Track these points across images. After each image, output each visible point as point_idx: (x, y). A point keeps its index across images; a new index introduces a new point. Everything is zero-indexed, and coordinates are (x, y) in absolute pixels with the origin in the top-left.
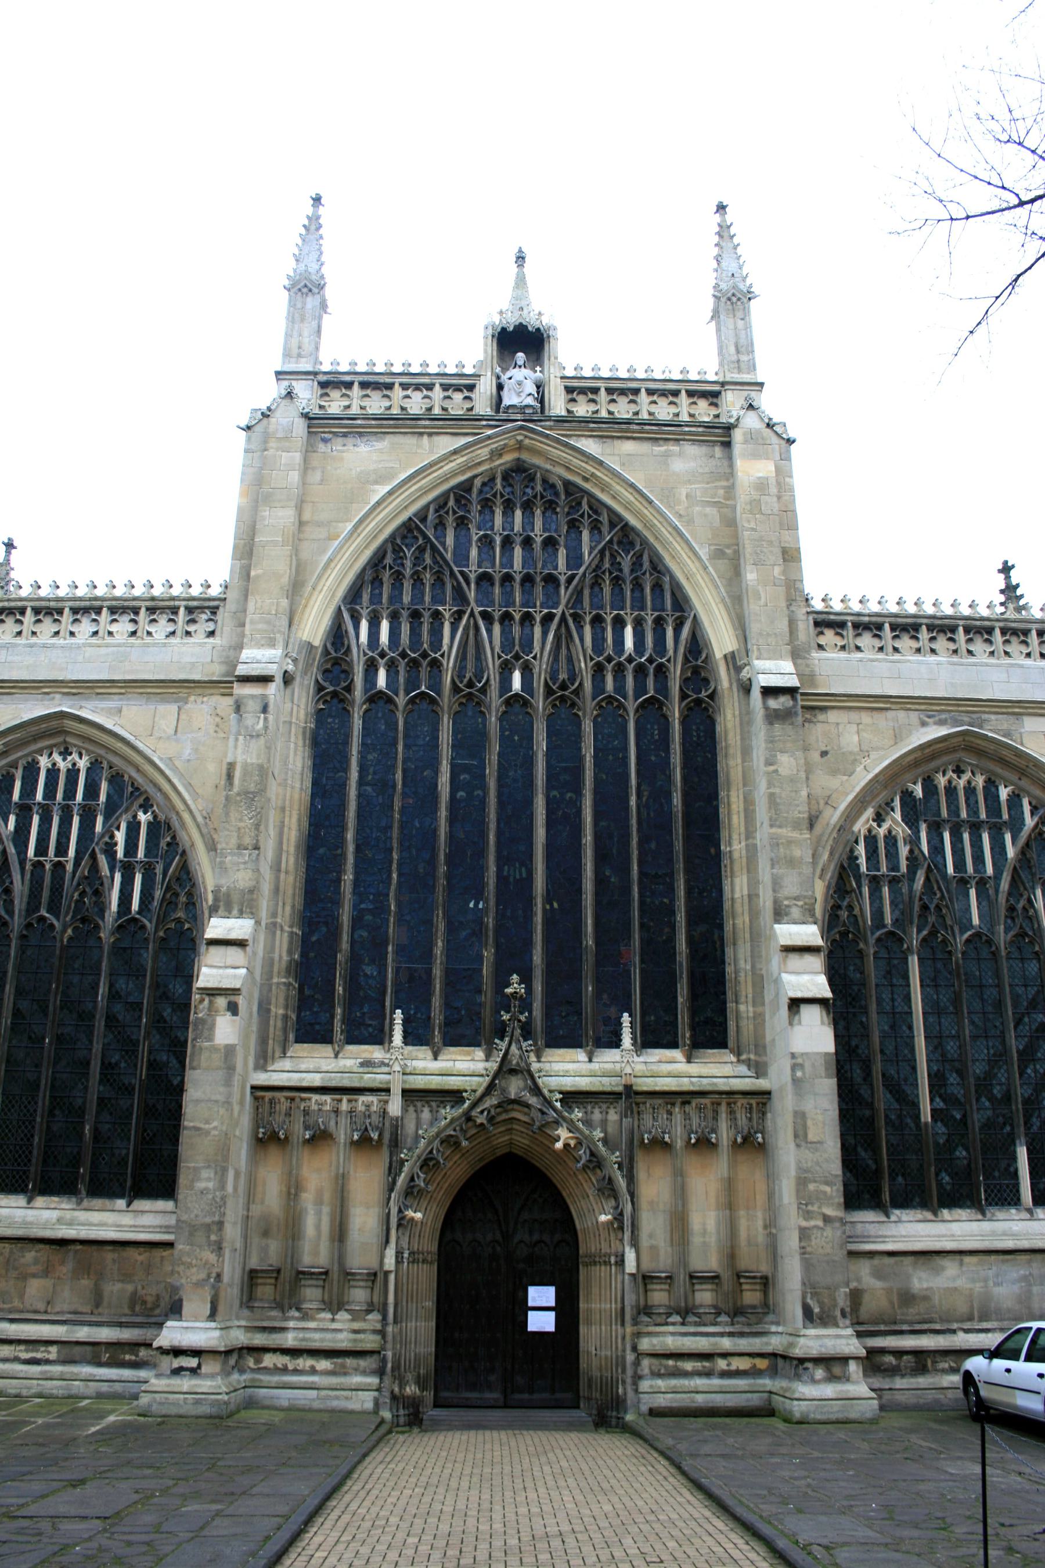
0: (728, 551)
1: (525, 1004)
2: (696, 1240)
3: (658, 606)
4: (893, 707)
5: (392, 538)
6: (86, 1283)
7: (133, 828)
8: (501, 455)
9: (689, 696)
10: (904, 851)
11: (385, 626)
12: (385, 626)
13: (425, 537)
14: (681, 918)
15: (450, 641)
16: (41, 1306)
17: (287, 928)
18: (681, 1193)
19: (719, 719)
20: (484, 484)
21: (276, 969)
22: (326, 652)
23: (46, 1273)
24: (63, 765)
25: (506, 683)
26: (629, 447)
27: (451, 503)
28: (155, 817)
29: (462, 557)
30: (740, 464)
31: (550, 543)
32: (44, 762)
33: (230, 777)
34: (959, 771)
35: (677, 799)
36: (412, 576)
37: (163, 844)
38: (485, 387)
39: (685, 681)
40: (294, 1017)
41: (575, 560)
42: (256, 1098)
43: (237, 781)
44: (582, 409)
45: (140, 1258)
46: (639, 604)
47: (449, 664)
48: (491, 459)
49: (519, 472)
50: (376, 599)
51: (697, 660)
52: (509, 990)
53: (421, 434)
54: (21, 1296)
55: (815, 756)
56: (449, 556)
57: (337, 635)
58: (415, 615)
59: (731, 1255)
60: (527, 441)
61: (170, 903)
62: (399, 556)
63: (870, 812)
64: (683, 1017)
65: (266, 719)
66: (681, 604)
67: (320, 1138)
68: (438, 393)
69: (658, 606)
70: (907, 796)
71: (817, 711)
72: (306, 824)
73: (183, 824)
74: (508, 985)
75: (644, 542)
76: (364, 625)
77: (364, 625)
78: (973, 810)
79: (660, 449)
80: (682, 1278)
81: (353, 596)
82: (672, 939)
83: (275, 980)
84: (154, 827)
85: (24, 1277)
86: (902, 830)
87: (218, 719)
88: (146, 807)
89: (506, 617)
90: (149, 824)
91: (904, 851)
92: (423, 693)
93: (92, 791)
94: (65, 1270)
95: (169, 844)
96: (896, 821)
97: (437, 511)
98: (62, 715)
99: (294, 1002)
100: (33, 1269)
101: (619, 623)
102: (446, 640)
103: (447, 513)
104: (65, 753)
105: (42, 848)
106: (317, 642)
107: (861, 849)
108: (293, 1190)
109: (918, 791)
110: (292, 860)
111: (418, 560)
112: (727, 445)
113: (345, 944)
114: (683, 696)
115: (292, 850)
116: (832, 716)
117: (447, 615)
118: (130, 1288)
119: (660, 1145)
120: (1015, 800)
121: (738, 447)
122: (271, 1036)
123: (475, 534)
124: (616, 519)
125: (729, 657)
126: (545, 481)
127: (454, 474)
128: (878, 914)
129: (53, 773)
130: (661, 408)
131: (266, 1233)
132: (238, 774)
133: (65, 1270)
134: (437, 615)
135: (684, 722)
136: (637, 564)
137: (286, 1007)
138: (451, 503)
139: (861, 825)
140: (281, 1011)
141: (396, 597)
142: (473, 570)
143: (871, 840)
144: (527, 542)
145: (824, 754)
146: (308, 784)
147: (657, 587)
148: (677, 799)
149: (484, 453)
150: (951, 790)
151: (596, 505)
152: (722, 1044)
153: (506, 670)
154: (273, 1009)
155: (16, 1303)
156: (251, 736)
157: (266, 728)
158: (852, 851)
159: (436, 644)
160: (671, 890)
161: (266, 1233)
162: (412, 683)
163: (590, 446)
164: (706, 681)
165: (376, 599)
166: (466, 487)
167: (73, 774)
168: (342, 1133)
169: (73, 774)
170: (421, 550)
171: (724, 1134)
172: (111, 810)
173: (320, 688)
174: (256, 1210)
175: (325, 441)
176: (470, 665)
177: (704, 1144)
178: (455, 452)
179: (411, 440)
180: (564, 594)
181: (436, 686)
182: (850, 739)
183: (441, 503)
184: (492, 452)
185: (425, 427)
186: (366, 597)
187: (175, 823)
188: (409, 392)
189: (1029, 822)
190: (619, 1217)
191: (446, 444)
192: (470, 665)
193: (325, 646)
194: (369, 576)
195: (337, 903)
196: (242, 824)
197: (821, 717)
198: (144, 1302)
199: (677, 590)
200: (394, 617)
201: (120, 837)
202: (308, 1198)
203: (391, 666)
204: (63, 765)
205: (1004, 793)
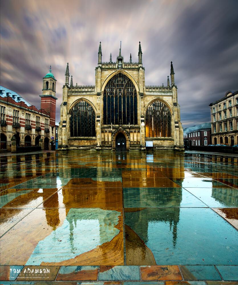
1: (121, 122)
2: (135, 139)
3: (132, 87)
5: (109, 81)
6: (90, 143)
7: (89, 107)
10: (152, 108)
11: (109, 89)
12: (109, 89)
14: (134, 114)
15: (114, 91)
18: (133, 136)
22: (104, 92)
23: (87, 142)
24: (83, 102)
25: (119, 94)
29: (115, 83)
30: (140, 73)
31: (123, 81)
32: (81, 102)
33: (97, 104)
34: (158, 101)
38: (117, 65)
39: (134, 94)
41: (125, 83)
42: (101, 129)
44: (126, 67)
46: (131, 87)
47: (114, 93)
49: (120, 74)
50: (108, 87)
55: (145, 100)
57: (105, 90)
58: (111, 88)
59: (137, 140)
61: (93, 114)
62: (110, 83)
63: (150, 105)
64: (134, 122)
66: (134, 86)
67: (106, 132)
69: (132, 87)
70: (153, 104)
76: (107, 89)
77: (107, 89)
78: (159, 105)
79: (133, 71)
80: (133, 142)
81: (106, 87)
82: (133, 116)
84: (91, 107)
85: (85, 143)
86: (152, 107)
88: (90, 106)
89: (119, 88)
91: (152, 108)
93: (85, 104)
96: (152, 106)
98: (82, 98)
101: (129, 88)
104: (83, 101)
105: (82, 110)
107: (149, 108)
108: (104, 136)
109: (154, 103)
111: (111, 83)
112: (139, 71)
113: (107, 117)
116: (147, 97)
119: (132, 132)
120: (162, 104)
121: (140, 72)
123: (116, 80)
124: (129, 78)
128: (150, 114)
129: (82, 103)
131: (103, 139)
133: (88, 142)
134: (113, 88)
135: (134, 97)
136: (130, 83)
139: (149, 107)
141: (110, 86)
142: (116, 84)
143: (150, 107)
144: (121, 81)
147: (132, 85)
149: (117, 72)
150: (157, 103)
151: (127, 77)
153: (119, 93)
159: (113, 91)
160: (133, 112)
161: (103, 139)
163: (126, 71)
164: (136, 94)
165: (108, 87)
166: (115, 75)
167: (84, 103)
168: (108, 131)
169: (84, 103)
171: (137, 131)
172: (87, 106)
173: (104, 95)
174: (102, 137)
177: (135, 132)
179: (110, 71)
180: (124, 86)
181: (113, 95)
182: (148, 99)
183: (113, 77)
189: (163, 106)
190: (129, 137)
191: (114, 71)
195: (106, 113)
199: (134, 85)
200: (110, 88)
201: (88, 108)
202: (106, 137)
203: (110, 93)
204: (83, 102)
205: (161, 103)
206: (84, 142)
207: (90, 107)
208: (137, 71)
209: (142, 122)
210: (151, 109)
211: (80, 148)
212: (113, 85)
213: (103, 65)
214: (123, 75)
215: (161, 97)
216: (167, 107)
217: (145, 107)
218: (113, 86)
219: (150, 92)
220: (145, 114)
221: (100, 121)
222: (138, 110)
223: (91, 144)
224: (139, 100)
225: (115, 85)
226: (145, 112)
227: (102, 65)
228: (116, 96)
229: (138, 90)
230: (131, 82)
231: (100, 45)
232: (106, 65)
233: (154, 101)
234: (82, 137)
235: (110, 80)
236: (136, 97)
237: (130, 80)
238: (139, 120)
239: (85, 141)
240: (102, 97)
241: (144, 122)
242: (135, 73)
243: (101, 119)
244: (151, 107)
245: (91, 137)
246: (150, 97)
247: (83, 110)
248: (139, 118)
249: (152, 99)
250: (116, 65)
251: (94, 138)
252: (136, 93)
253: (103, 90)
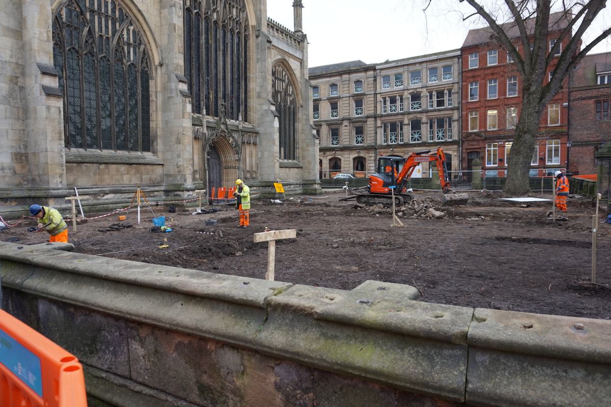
6: (138, 175)
16: (128, 183)
23: (128, 173)
43: (177, 31)
45: (150, 168)
54: (122, 180)
85: (122, 175)
94: (133, 171)
100: (125, 172)
118: (149, 176)
132: (176, 28)
133: (133, 171)
155: (122, 183)
198: (152, 180)
205: (284, 73)
206: (118, 170)
207: (132, 28)
211: (106, 197)
215: (287, 58)
223: (141, 179)
228: (207, 19)
229: (252, 22)
234: (106, 152)
239: (123, 168)
245: (139, 153)
247: (101, 31)
251: (148, 156)
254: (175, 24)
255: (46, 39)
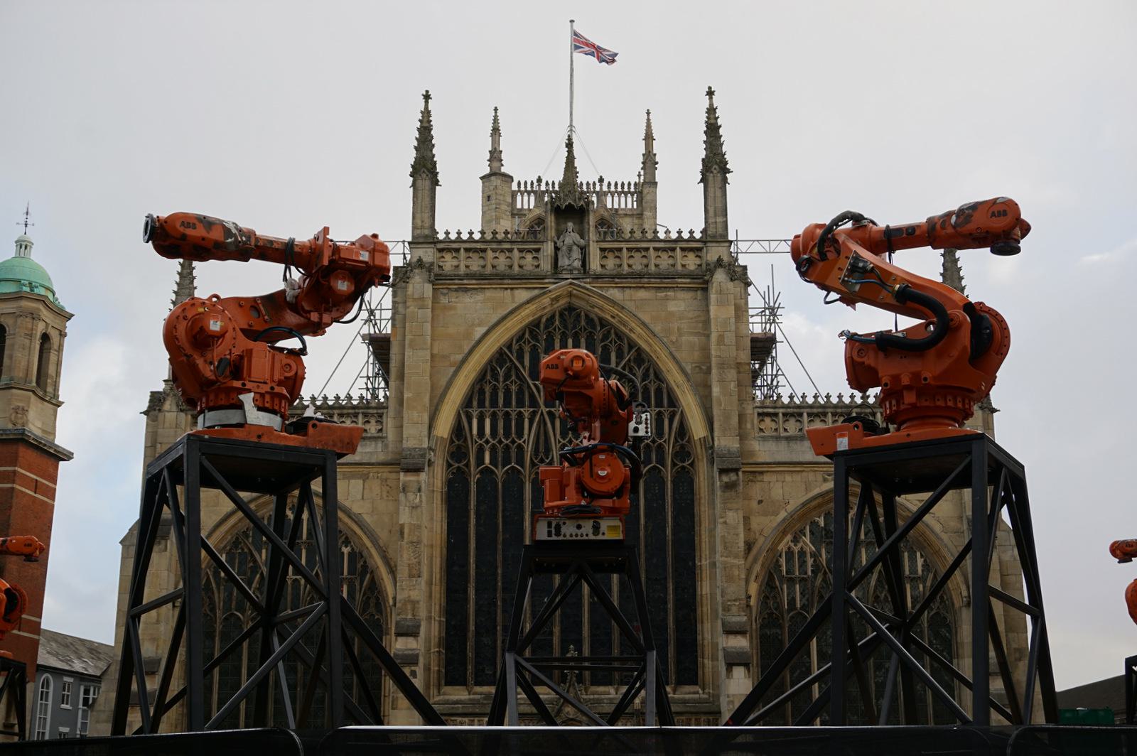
0: (703, 367)
4: (806, 469)
5: (490, 362)
8: (558, 301)
9: (677, 465)
10: (810, 561)
11: (488, 422)
12: (488, 422)
13: (511, 360)
14: (670, 606)
17: (437, 618)
19: (696, 480)
20: (547, 320)
21: (432, 644)
22: (452, 441)
26: (642, 294)
27: (527, 336)
28: (353, 549)
30: (713, 309)
35: (669, 531)
36: (503, 388)
37: (359, 566)
39: (675, 455)
40: (444, 671)
43: (406, 536)
48: (552, 304)
51: (682, 440)
52: (569, 655)
53: (506, 289)
55: (754, 504)
56: (526, 375)
57: (458, 431)
60: (575, 292)
62: (495, 376)
63: (789, 537)
65: (420, 496)
66: (673, 402)
68: (516, 253)
71: (757, 474)
72: (445, 551)
73: (371, 556)
74: (568, 652)
75: (650, 360)
81: (467, 403)
82: (665, 619)
83: (432, 651)
87: (388, 488)
90: (349, 554)
91: (810, 561)
92: (513, 466)
95: (362, 566)
97: (517, 341)
99: (443, 662)
102: (526, 431)
103: (524, 343)
106: (446, 436)
107: (783, 561)
110: (438, 576)
111: (507, 377)
112: (705, 290)
114: (674, 464)
115: (438, 570)
116: (766, 478)
117: (526, 414)
121: (713, 297)
122: (432, 683)
124: (632, 345)
125: (702, 440)
126: (587, 316)
127: (528, 316)
128: (792, 602)
130: (664, 260)
132: (406, 531)
134: (520, 415)
136: (646, 376)
137: (439, 666)
138: (527, 336)
139: (782, 547)
140: (436, 668)
141: (494, 403)
145: (760, 502)
146: (445, 527)
147: (659, 391)
148: (669, 531)
149: (546, 300)
151: (619, 335)
152: (695, 683)
154: (432, 668)
156: (413, 507)
157: (421, 501)
158: (777, 561)
159: (520, 435)
160: (666, 588)
162: (506, 461)
163: (614, 294)
164: (689, 455)
170: (509, 369)
173: (449, 465)
175: (444, 295)
176: (542, 449)
178: (528, 302)
181: (522, 464)
182: (777, 492)
183: (520, 337)
184: (552, 300)
185: (508, 284)
186: (475, 403)
187: (365, 553)
188: (497, 254)
192: (542, 449)
193: (451, 437)
194: (477, 387)
195: (466, 600)
196: (411, 562)
197: (759, 478)
208: (689, 289)
209: (730, 666)
210: (803, 563)
212: (520, 393)
213: (449, 250)
214: (590, 321)
216: (922, 548)
217: (754, 551)
218: (520, 403)
219: (788, 439)
220: (753, 602)
221: (416, 664)
222: (706, 574)
224: (712, 504)
225: (532, 396)
226: (754, 589)
227: (441, 250)
229: (698, 429)
230: (648, 370)
231: (426, 113)
232: (467, 250)
233: (819, 506)
235: (500, 357)
236: (685, 480)
237: (641, 357)
238: (708, 651)
240: (434, 478)
241: (746, 665)
242: (680, 303)
243: (428, 640)
244: (802, 553)
246: (788, 478)
248: (708, 636)
249: (807, 490)
250: (538, 250)
252: (683, 452)
253: (444, 427)
254: (402, 526)
255: (154, 621)
